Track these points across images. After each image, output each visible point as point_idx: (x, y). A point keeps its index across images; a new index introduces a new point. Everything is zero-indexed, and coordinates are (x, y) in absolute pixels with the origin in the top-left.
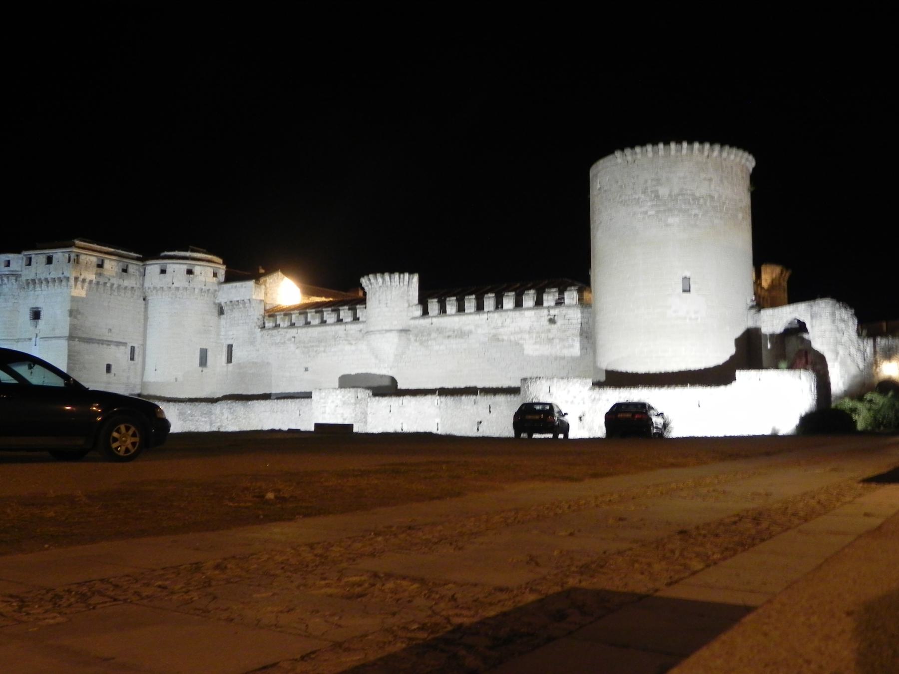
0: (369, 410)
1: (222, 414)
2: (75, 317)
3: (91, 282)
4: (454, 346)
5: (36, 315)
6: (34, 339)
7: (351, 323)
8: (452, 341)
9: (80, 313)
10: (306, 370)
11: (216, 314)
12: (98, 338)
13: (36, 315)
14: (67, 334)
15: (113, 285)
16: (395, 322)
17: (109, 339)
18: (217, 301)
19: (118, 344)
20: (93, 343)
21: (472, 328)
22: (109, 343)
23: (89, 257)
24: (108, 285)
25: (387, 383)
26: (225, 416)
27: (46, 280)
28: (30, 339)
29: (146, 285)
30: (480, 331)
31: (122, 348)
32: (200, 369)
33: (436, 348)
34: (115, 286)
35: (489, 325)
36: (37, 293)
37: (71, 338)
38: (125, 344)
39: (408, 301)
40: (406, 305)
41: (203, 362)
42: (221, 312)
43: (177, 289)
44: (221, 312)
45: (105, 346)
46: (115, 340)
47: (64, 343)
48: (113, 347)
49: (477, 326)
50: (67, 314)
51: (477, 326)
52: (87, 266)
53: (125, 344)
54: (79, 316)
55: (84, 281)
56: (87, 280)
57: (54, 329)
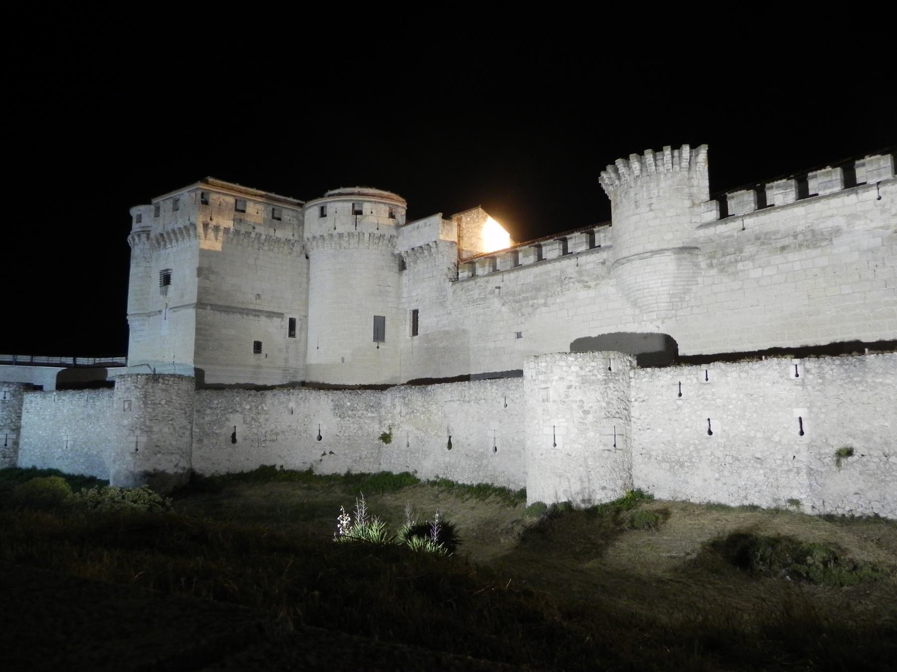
0: (633, 394)
1: (394, 406)
2: (207, 278)
3: (227, 230)
4: (797, 266)
5: (166, 279)
6: (164, 311)
7: (586, 252)
8: (791, 256)
9: (213, 272)
10: (519, 335)
11: (396, 269)
12: (240, 306)
13: (166, 279)
14: (195, 301)
15: (259, 235)
16: (669, 236)
17: (257, 308)
18: (396, 252)
19: (271, 315)
20: (234, 313)
21: (841, 222)
22: (257, 313)
23: (222, 198)
24: (253, 235)
25: (658, 347)
26: (398, 409)
27: (173, 231)
28: (160, 312)
29: (305, 236)
30: (860, 225)
31: (277, 321)
32: (376, 344)
33: (756, 273)
34: (263, 237)
35: (883, 211)
36: (167, 251)
37: (200, 305)
38: (280, 315)
39: (691, 196)
40: (688, 203)
41: (379, 334)
42: (403, 266)
43: (341, 235)
44: (403, 266)
45: (251, 317)
46: (265, 309)
47: (192, 312)
48: (263, 319)
49: (853, 217)
50: (195, 272)
51: (853, 217)
52: (220, 209)
53: (280, 315)
54: (212, 277)
55: (217, 228)
56: (222, 228)
57: (182, 296)
